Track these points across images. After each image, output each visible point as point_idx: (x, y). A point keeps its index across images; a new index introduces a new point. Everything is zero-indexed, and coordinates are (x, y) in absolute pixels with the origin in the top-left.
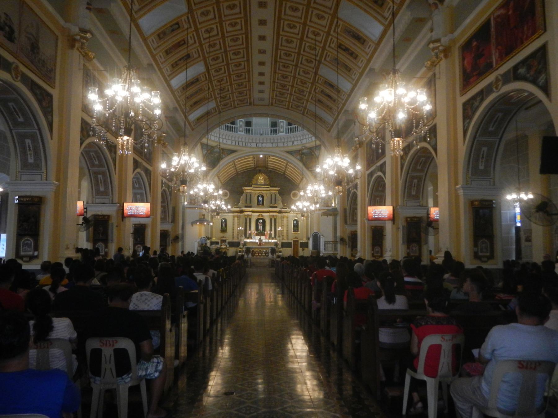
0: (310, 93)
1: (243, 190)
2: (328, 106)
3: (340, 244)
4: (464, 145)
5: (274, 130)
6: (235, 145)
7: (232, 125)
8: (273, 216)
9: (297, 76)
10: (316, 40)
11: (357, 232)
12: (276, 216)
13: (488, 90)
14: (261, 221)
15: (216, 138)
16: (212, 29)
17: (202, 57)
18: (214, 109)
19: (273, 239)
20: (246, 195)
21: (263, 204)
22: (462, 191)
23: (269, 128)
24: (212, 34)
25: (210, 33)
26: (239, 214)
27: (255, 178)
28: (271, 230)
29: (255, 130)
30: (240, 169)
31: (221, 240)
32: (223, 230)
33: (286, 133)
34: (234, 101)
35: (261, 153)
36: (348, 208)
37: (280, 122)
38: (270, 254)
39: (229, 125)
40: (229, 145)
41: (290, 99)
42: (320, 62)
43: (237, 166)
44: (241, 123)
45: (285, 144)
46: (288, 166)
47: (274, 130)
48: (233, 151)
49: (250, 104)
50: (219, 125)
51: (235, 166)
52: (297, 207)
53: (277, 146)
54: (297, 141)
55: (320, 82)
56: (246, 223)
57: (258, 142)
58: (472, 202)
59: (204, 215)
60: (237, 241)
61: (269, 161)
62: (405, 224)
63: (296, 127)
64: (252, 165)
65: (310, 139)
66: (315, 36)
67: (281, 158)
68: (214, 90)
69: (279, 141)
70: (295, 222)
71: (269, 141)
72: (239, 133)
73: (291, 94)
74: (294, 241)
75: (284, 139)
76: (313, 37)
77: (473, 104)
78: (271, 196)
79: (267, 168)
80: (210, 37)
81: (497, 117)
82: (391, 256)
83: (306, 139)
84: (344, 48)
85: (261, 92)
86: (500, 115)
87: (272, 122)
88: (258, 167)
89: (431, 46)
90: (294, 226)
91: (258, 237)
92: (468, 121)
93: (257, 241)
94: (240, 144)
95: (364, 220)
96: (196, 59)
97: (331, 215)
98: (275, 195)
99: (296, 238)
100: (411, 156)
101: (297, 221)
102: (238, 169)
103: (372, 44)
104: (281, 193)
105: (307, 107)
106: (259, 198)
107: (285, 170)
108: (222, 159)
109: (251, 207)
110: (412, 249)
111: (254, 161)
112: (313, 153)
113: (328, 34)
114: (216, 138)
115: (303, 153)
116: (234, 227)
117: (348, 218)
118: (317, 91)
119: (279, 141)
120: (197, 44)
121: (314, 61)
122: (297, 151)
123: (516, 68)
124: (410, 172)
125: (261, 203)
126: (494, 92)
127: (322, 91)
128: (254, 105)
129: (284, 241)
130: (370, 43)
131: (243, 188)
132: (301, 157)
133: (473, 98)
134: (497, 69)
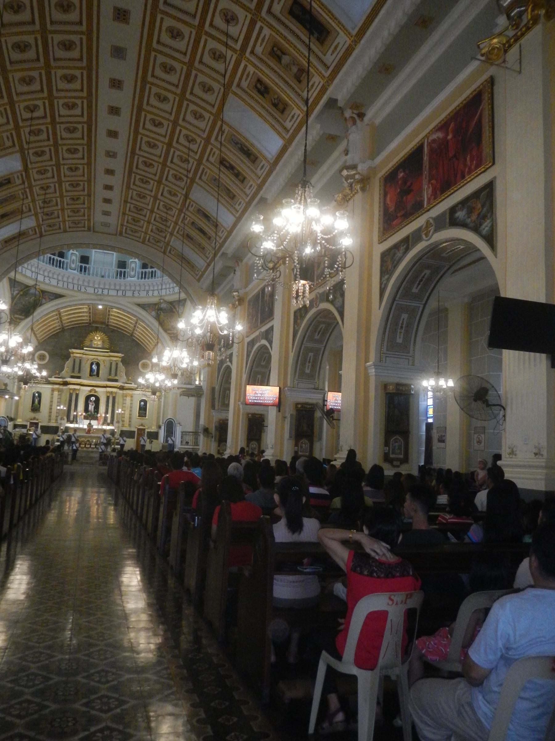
0: (176, 223)
1: (70, 353)
2: (200, 245)
3: (204, 436)
4: (379, 309)
5: (121, 272)
6: (63, 288)
7: (59, 259)
8: (112, 393)
9: (159, 196)
10: (189, 149)
11: (228, 420)
12: (116, 393)
13: (416, 237)
14: (93, 399)
15: (34, 274)
16: (36, 107)
17: (17, 148)
18: (33, 229)
19: (108, 425)
20: (74, 360)
21: (98, 375)
22: (374, 370)
23: (114, 269)
24: (35, 114)
25: (32, 111)
26: (61, 387)
27: (90, 337)
28: (107, 412)
29: (94, 268)
30: (68, 323)
31: (31, 423)
32: (35, 408)
33: (138, 278)
34: (64, 221)
35: (99, 302)
36: (217, 388)
37: (131, 262)
39: (56, 258)
40: (53, 286)
41: (147, 228)
42: (193, 181)
43: (63, 318)
44: (74, 257)
45: (136, 294)
46: (138, 325)
47: (121, 272)
48: (58, 296)
49: (89, 229)
50: (37, 254)
51: (61, 318)
52: (147, 380)
53: (124, 296)
54: (153, 291)
55: (191, 209)
56: (70, 401)
57: (97, 286)
58: (385, 386)
59: (6, 385)
60: (54, 425)
61: (112, 315)
62: (294, 413)
63: (152, 272)
64: (85, 318)
65: (171, 290)
66: (189, 142)
67: (128, 312)
68: (34, 201)
69: (128, 288)
70: (142, 403)
71: (112, 287)
72: (69, 270)
73: (149, 222)
74: (138, 429)
76: (187, 144)
77: (394, 254)
78: (111, 363)
79: (108, 325)
80: (32, 119)
81: (423, 274)
82: (273, 455)
83: (166, 289)
84: (228, 165)
85: (106, 213)
86: (428, 272)
87: (119, 261)
88: (94, 322)
89: (345, 173)
90: (140, 408)
91: (87, 422)
92: (386, 277)
93: (85, 427)
94: (71, 286)
95: (239, 405)
96: (7, 148)
97: (193, 396)
98: (117, 364)
99: (142, 425)
100: (308, 321)
101: (145, 402)
102: (64, 322)
103: (266, 164)
104: (124, 361)
105: (171, 244)
106: (93, 366)
107: (134, 330)
108: (41, 305)
109: (79, 377)
110: (301, 447)
111: (90, 313)
112: (174, 310)
113: (207, 141)
114: (34, 274)
115: (160, 309)
116: (51, 406)
117: (217, 400)
118: (186, 222)
119: (128, 288)
120: (12, 126)
121: (185, 178)
122: (152, 304)
123: (453, 210)
124: (304, 342)
125: (95, 373)
126: (424, 240)
127: (193, 223)
128: (94, 231)
129: (124, 429)
130: (264, 162)
131: (70, 350)
132: (157, 313)
133: (396, 247)
134: (428, 210)
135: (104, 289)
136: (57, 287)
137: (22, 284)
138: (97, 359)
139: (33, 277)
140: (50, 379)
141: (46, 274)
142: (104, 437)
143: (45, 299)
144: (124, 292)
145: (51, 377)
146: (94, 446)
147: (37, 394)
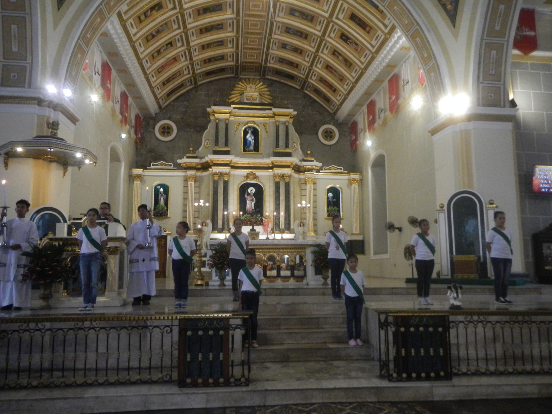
1: (209, 114)
8: (283, 176)
12: (290, 176)
14: (252, 190)
19: (282, 232)
20: (217, 125)
21: (256, 149)
26: (199, 174)
38: (310, 270)
56: (216, 193)
59: (54, 126)
70: (331, 195)
78: (277, 128)
90: (329, 204)
98: (287, 128)
106: (248, 136)
109: (227, 153)
125: (252, 148)
138: (254, 122)
140: (179, 161)
142: (338, 240)
145: (181, 158)
146: (288, 273)
147: (162, 190)
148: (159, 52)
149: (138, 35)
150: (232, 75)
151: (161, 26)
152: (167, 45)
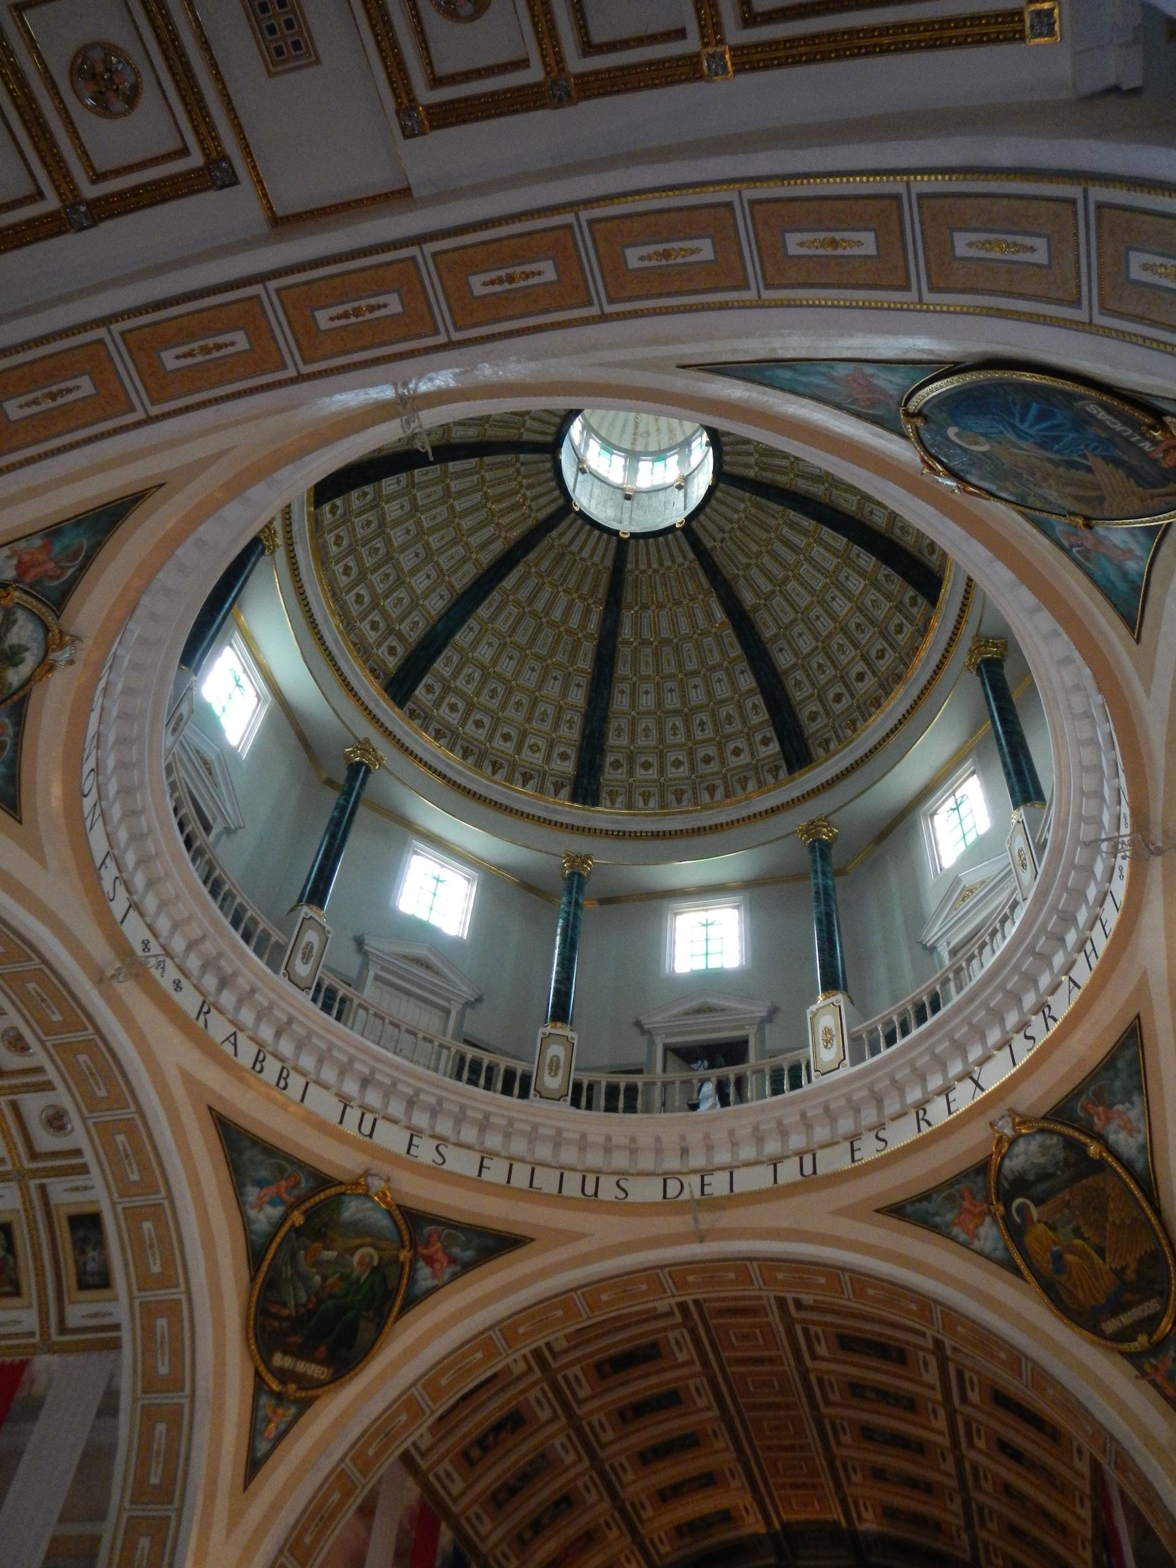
6: (506, 1190)
37: (815, 1014)
54: (946, 1091)
57: (672, 1163)
75: (856, 1110)
83: (1006, 1043)
108: (411, 1302)
112: (1093, 1149)
114: (353, 1115)
115: (1020, 1185)
122: (964, 1175)
132: (1007, 1217)
135: (711, 1172)
136: (477, 1184)
137: (300, 1165)
139: (350, 1127)
141: (420, 1119)
143: (430, 1261)
144: (808, 1159)
148: (537, 1526)
149: (466, 1500)
150: (772, 1560)
151: (531, 1463)
152: (557, 1504)
